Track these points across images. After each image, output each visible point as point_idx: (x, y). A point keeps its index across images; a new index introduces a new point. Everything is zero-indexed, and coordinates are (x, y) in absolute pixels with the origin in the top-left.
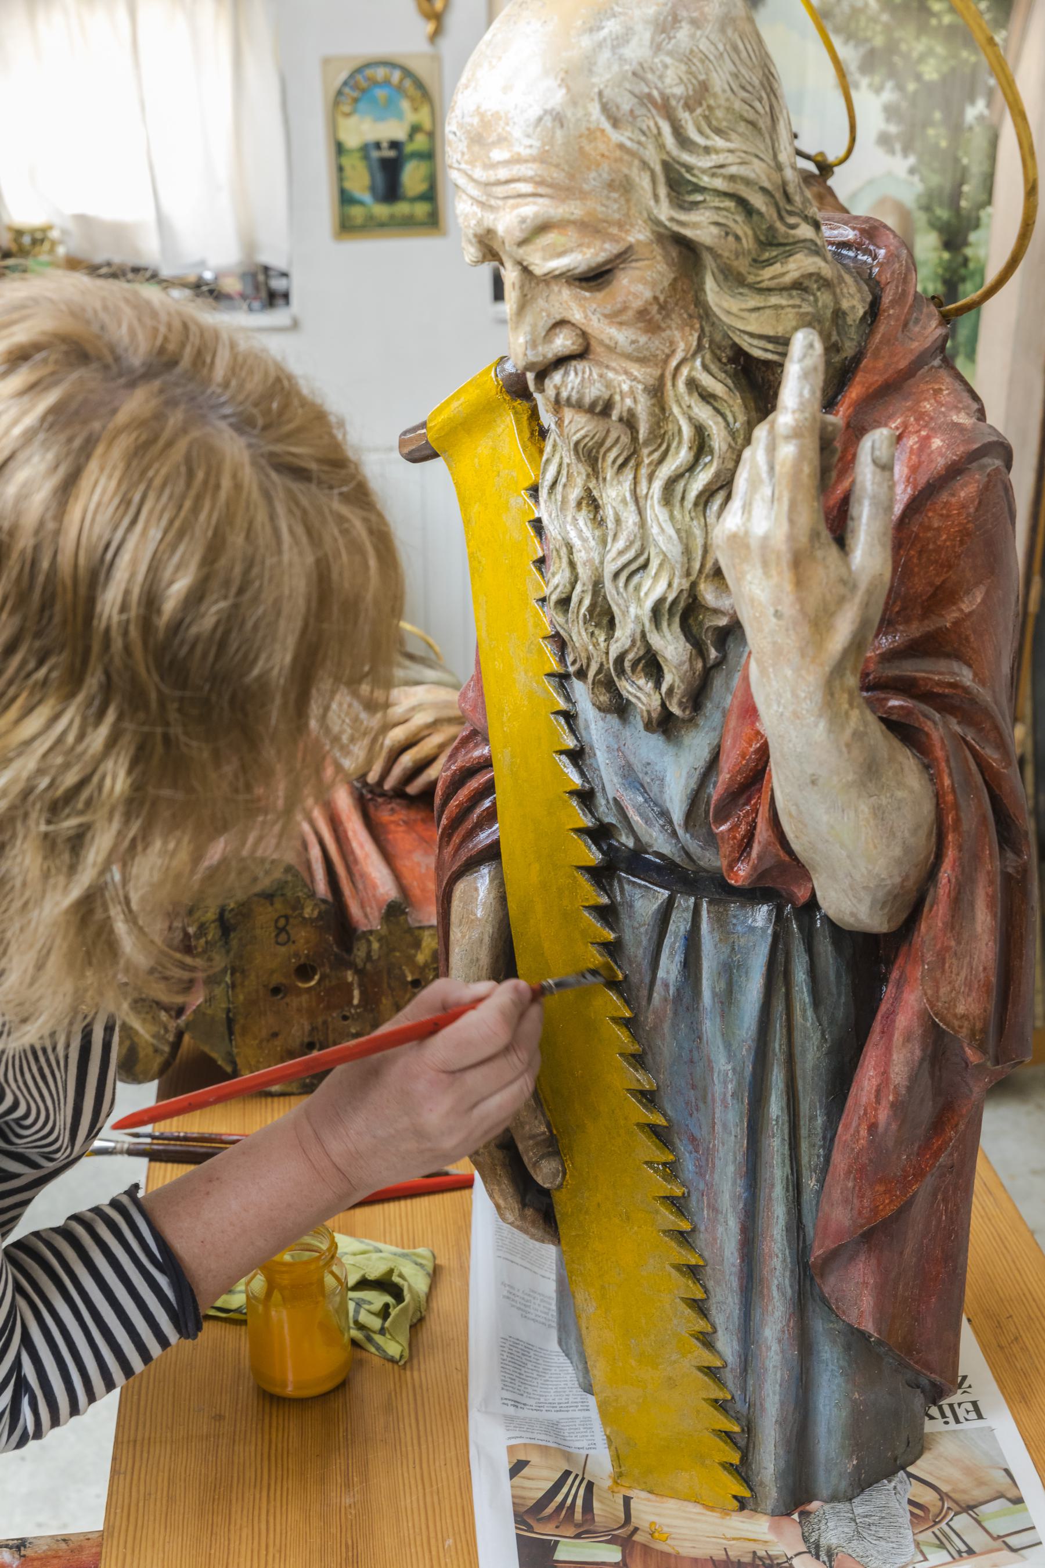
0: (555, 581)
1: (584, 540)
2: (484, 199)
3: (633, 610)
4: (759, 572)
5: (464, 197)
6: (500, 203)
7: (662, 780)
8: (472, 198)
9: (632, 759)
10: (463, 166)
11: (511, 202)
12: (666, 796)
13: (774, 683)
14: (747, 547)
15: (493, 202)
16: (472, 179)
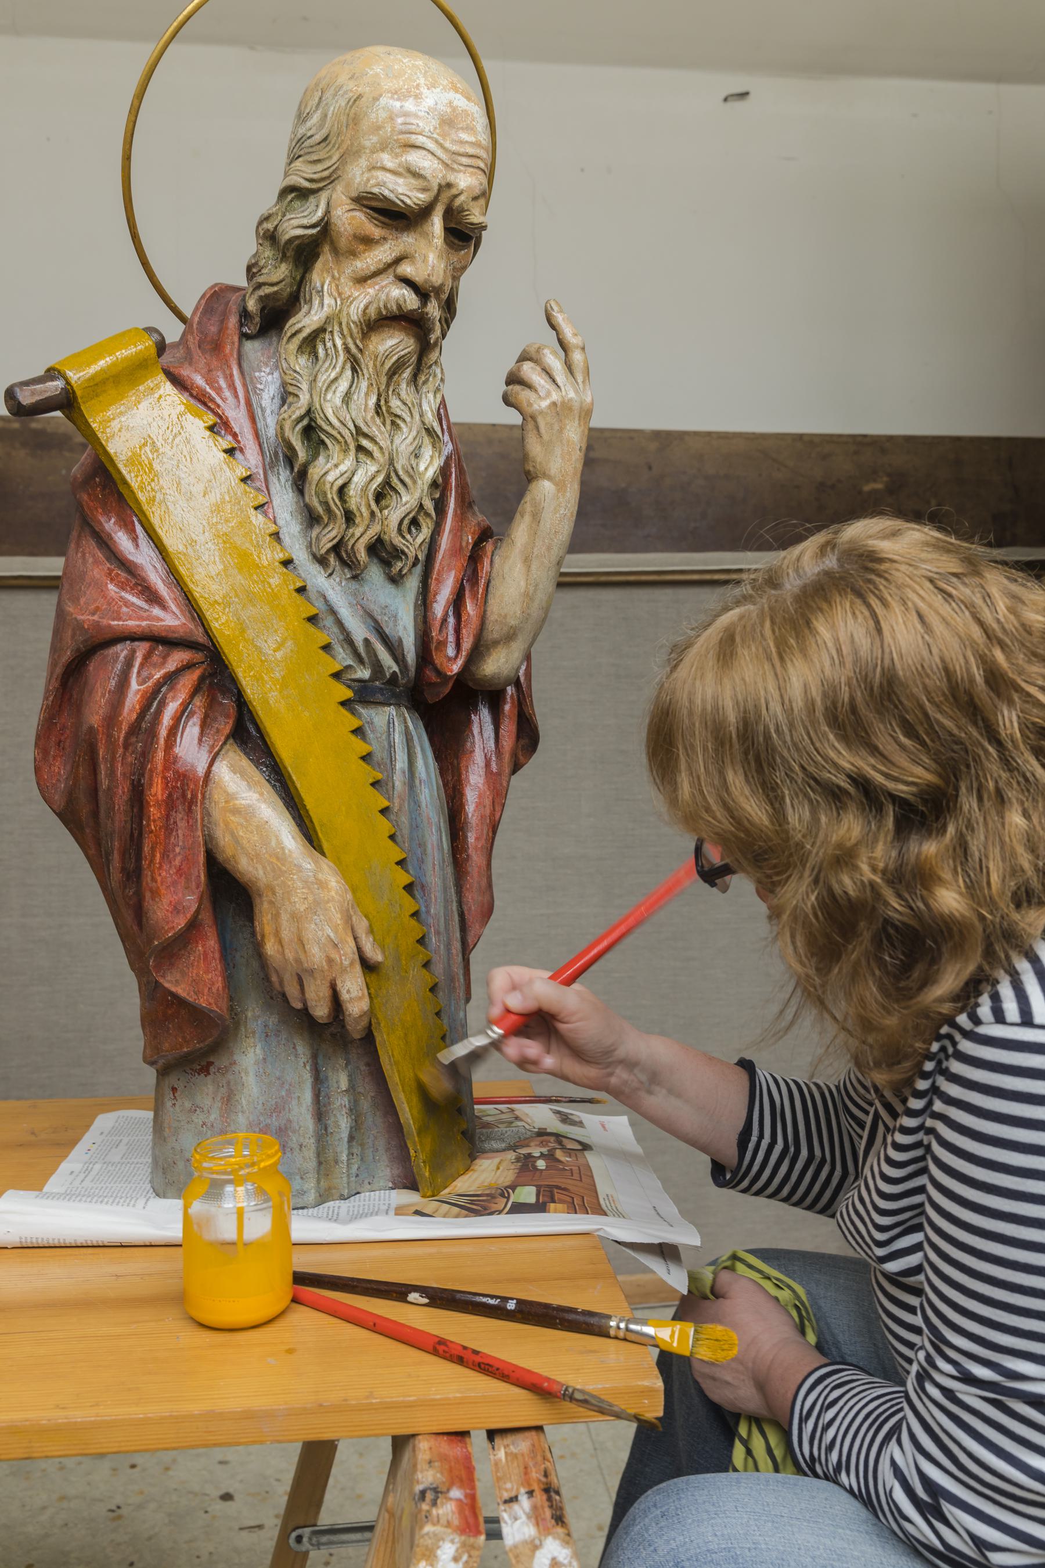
0: (343, 468)
1: (382, 433)
2: (449, 162)
3: (419, 482)
4: (577, 422)
5: (430, 157)
6: (462, 168)
7: (395, 617)
8: (439, 159)
9: (372, 606)
10: (435, 136)
11: (472, 170)
12: (400, 628)
13: (568, 494)
14: (570, 409)
15: (455, 166)
16: (442, 146)
